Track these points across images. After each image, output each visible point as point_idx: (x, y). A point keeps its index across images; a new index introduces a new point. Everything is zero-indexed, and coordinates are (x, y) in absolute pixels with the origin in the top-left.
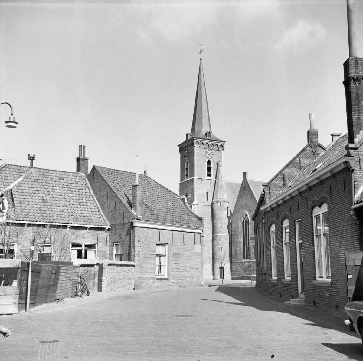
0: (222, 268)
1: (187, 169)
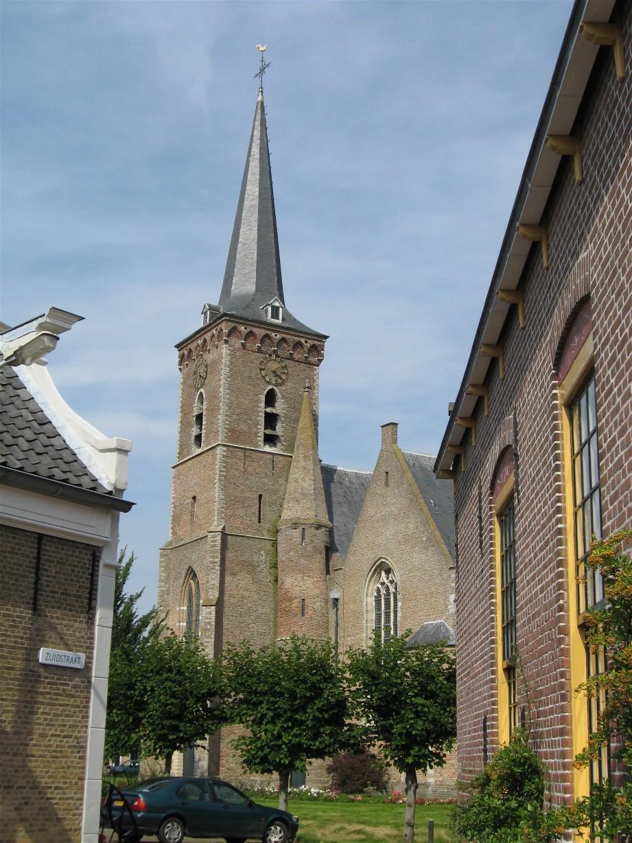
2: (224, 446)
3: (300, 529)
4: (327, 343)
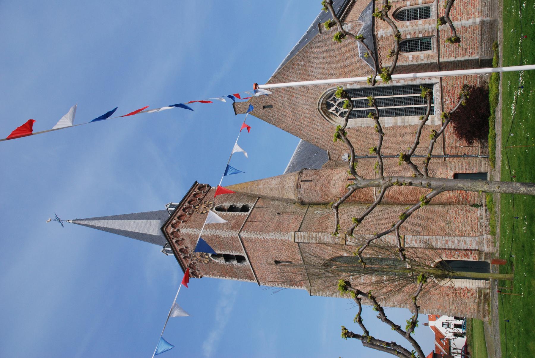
1: (228, 258)
2: (240, 231)
3: (302, 184)
4: (199, 182)
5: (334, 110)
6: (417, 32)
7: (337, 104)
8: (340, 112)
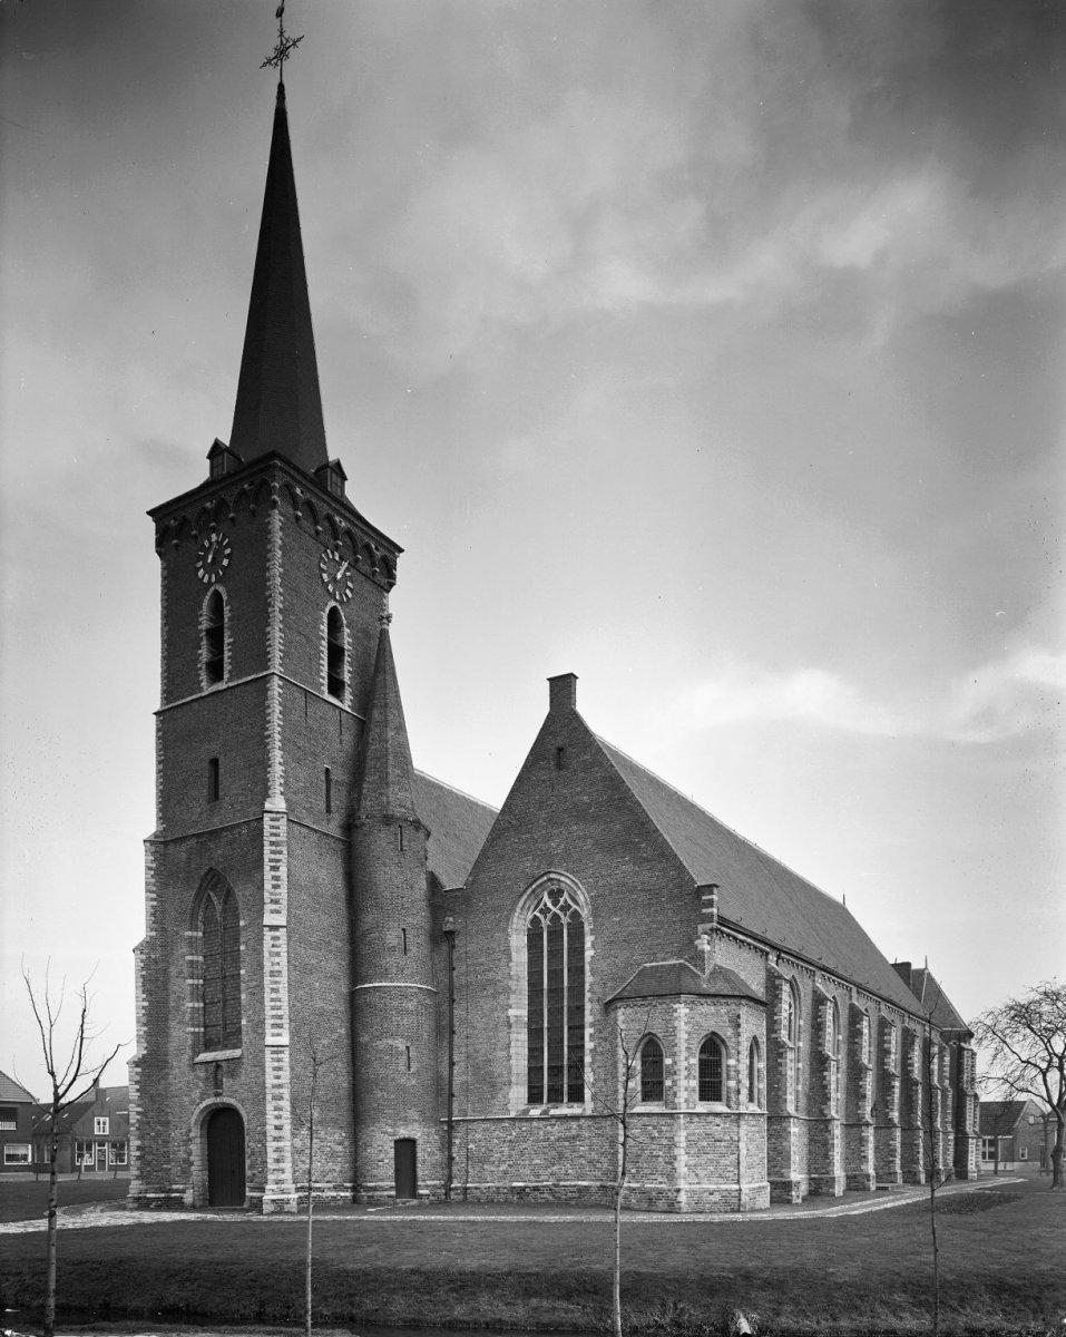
0: (406, 1148)
5: (545, 904)
6: (676, 1077)
7: (558, 912)
8: (541, 917)
